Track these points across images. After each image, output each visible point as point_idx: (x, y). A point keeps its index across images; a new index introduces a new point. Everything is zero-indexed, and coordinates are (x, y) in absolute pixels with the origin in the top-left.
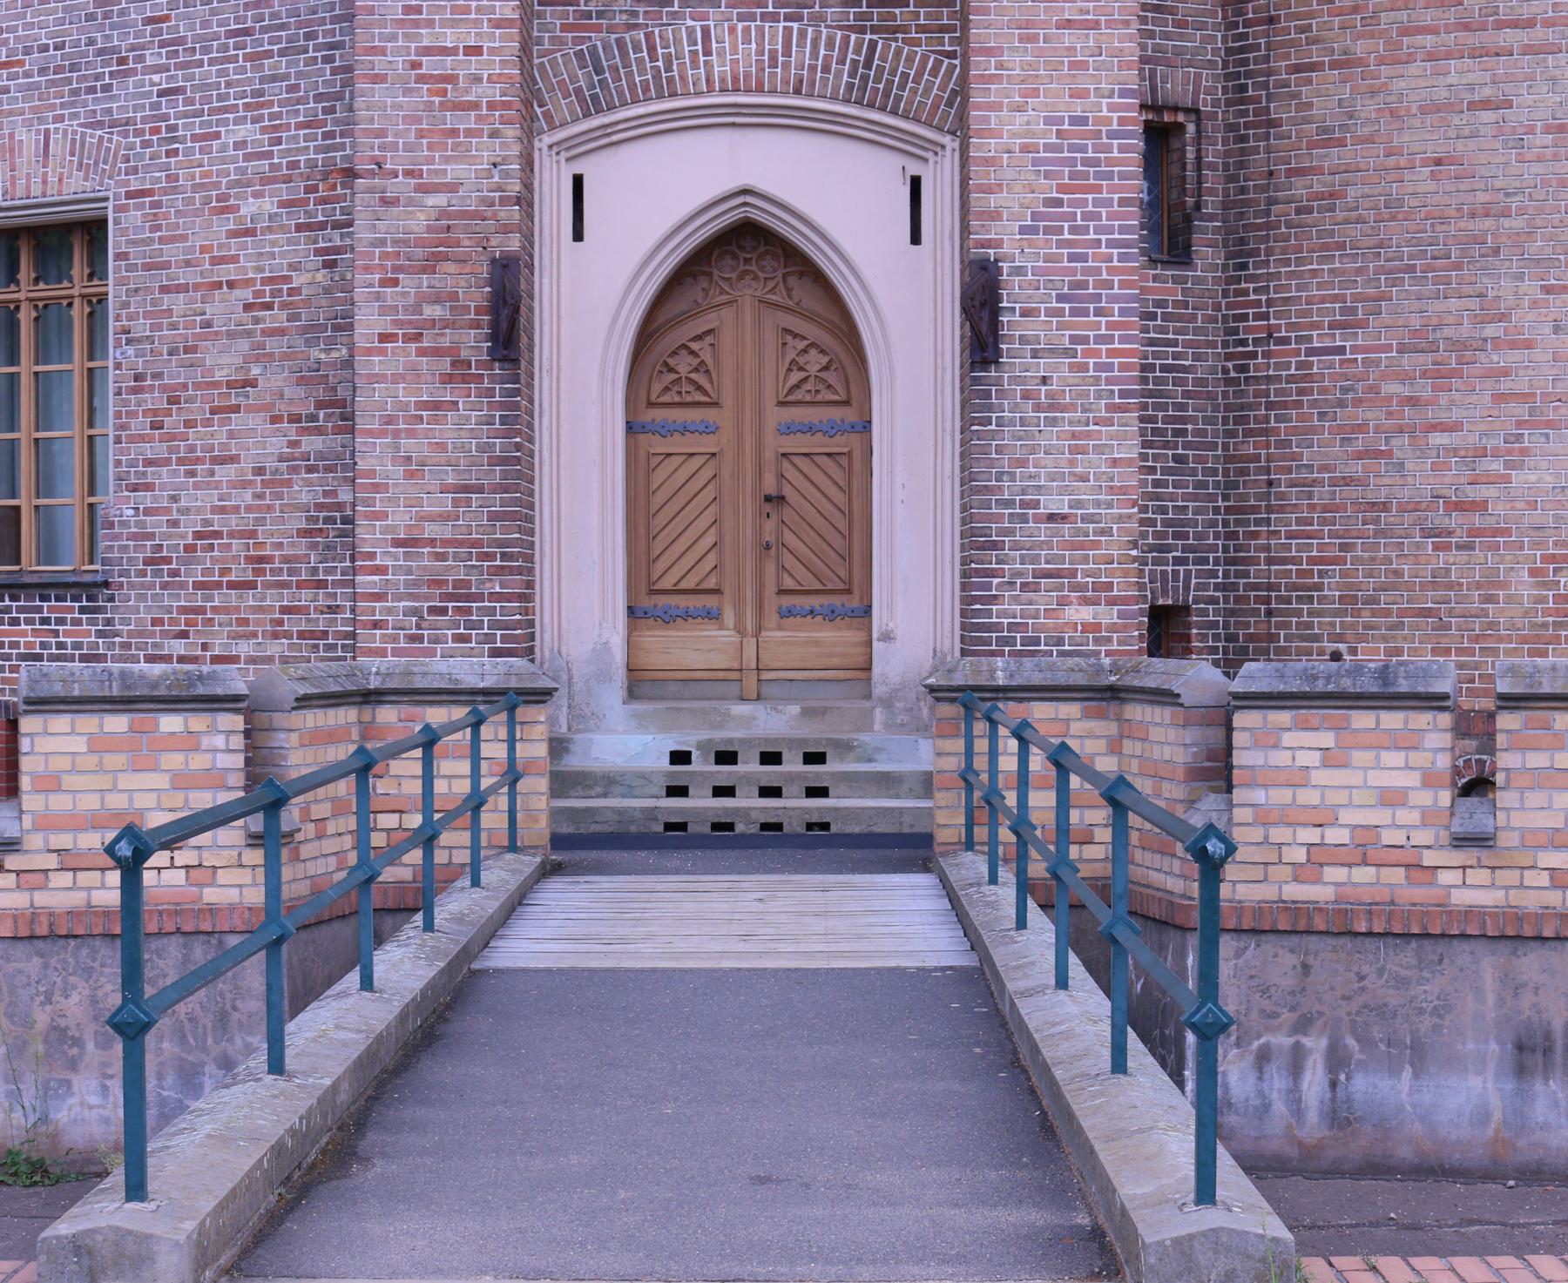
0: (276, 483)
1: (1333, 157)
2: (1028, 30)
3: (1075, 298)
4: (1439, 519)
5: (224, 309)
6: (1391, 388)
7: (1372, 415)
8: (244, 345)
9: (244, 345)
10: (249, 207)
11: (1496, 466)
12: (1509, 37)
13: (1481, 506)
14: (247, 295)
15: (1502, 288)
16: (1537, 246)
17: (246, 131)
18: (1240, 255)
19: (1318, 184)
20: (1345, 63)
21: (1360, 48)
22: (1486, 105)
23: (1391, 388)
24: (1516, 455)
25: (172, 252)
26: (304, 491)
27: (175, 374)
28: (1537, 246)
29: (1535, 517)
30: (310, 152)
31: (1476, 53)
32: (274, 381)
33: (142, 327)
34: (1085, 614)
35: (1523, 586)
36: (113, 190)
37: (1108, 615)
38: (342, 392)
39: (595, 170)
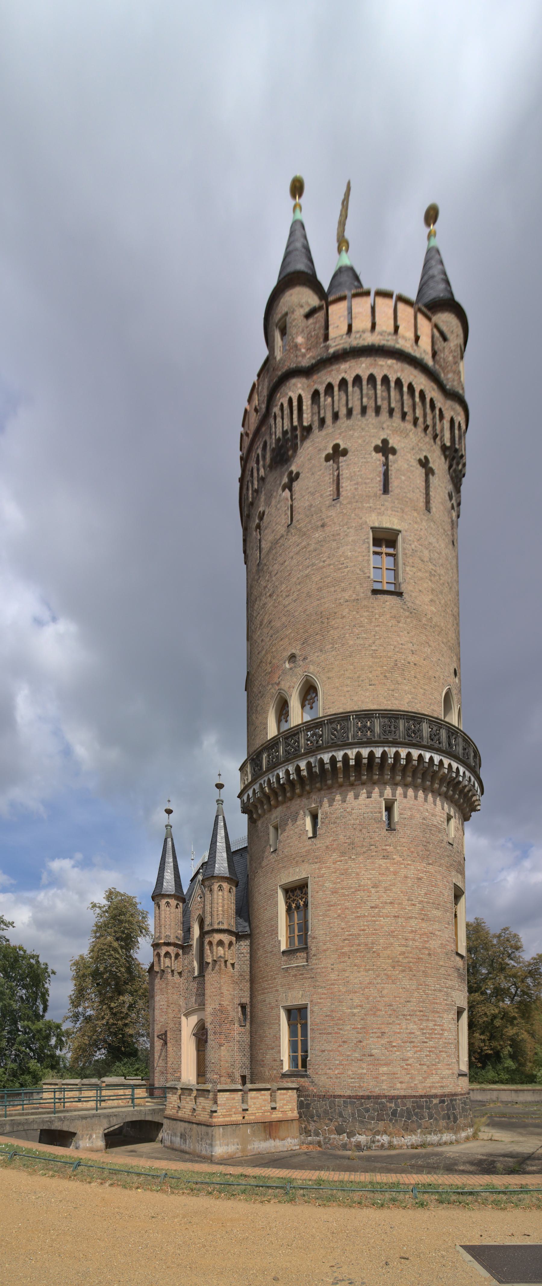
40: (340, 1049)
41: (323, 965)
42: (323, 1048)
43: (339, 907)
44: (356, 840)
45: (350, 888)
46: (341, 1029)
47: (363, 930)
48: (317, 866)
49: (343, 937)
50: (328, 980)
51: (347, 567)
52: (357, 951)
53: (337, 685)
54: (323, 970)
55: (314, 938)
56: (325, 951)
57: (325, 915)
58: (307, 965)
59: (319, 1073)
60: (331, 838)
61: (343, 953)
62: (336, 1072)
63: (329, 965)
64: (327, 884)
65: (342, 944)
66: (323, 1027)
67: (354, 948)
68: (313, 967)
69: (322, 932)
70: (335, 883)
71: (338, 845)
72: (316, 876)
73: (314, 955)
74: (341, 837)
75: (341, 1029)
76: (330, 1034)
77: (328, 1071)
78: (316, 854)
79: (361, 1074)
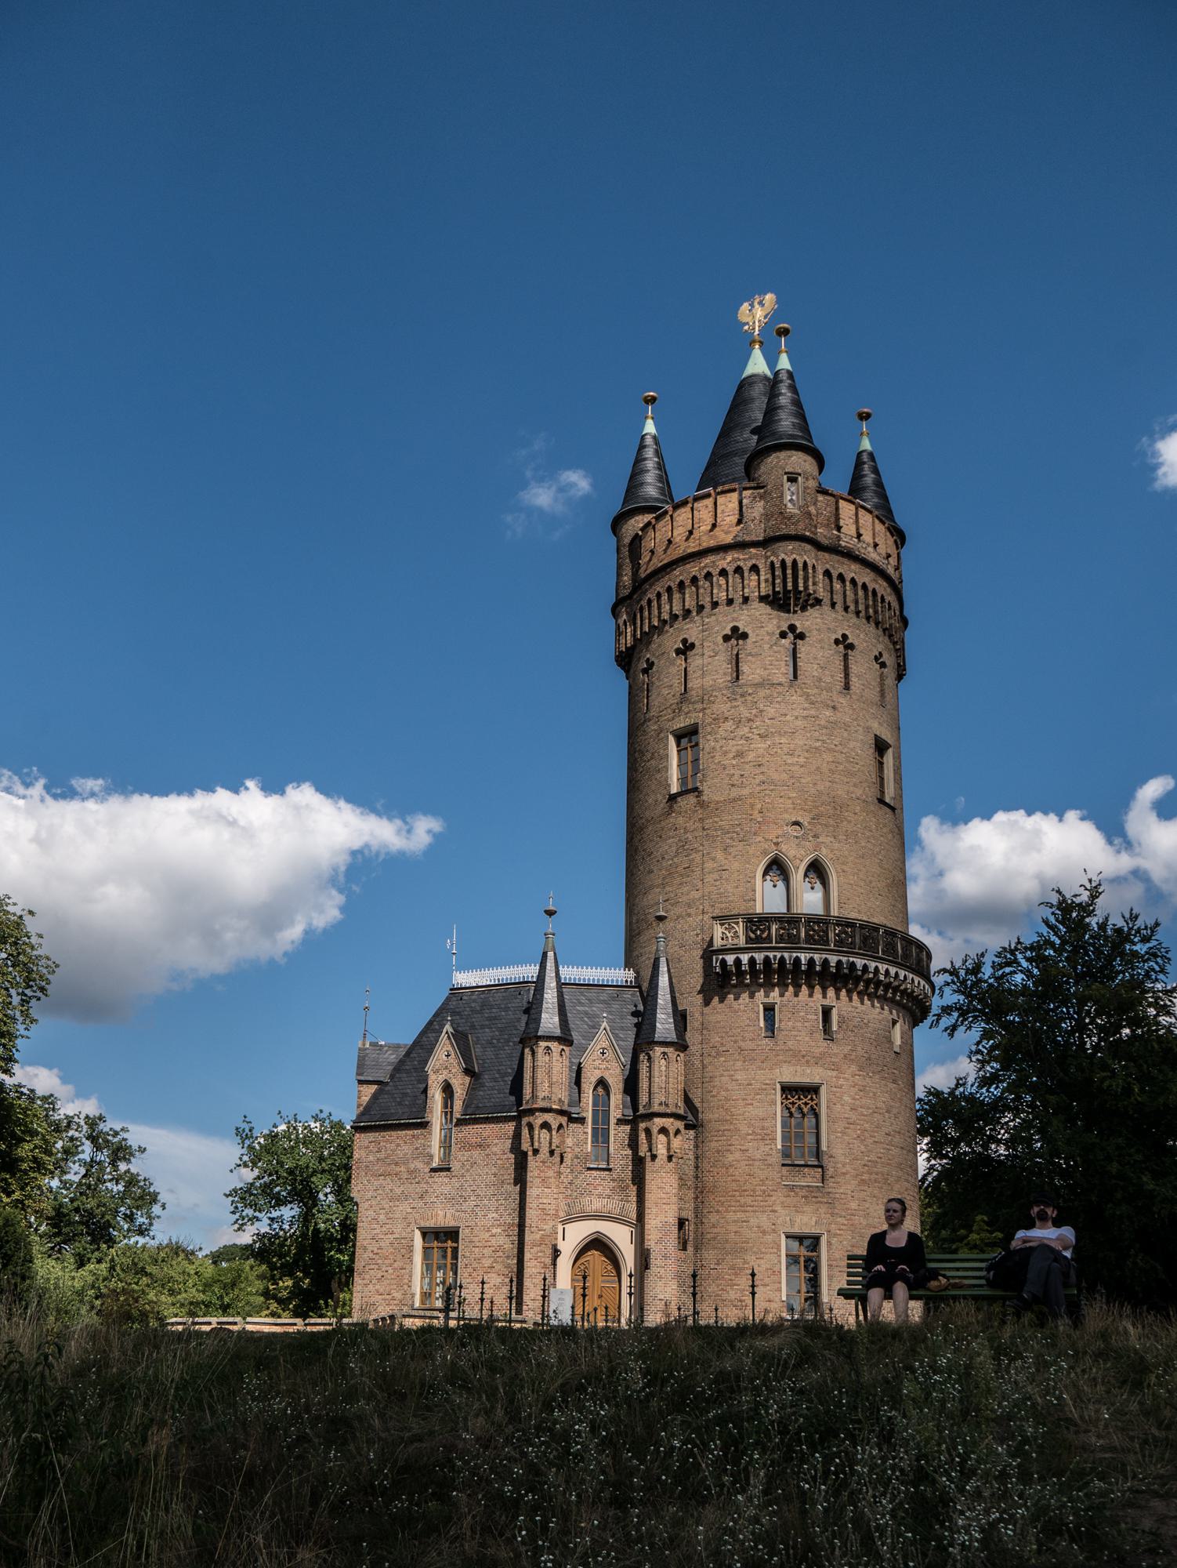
1: (715, 1230)
2: (656, 1204)
4: (736, 1303)
5: (487, 1252)
10: (494, 1231)
16: (755, 1249)
18: (697, 1249)
20: (718, 1211)
22: (745, 1221)
25: (475, 1239)
27: (475, 1265)
28: (755, 1249)
32: (498, 1267)
33: (468, 1254)
36: (461, 1225)
41: (842, 1191)
43: (859, 1127)
44: (873, 1056)
45: (869, 1108)
47: (881, 1158)
48: (834, 1073)
49: (863, 1162)
51: (857, 764)
52: (876, 1181)
54: (843, 1196)
55: (831, 1157)
56: (844, 1174)
57: (843, 1133)
61: (863, 1180)
64: (846, 1098)
67: (874, 1176)
68: (830, 1190)
69: (841, 1151)
71: (857, 1056)
73: (832, 1177)
74: (859, 1049)
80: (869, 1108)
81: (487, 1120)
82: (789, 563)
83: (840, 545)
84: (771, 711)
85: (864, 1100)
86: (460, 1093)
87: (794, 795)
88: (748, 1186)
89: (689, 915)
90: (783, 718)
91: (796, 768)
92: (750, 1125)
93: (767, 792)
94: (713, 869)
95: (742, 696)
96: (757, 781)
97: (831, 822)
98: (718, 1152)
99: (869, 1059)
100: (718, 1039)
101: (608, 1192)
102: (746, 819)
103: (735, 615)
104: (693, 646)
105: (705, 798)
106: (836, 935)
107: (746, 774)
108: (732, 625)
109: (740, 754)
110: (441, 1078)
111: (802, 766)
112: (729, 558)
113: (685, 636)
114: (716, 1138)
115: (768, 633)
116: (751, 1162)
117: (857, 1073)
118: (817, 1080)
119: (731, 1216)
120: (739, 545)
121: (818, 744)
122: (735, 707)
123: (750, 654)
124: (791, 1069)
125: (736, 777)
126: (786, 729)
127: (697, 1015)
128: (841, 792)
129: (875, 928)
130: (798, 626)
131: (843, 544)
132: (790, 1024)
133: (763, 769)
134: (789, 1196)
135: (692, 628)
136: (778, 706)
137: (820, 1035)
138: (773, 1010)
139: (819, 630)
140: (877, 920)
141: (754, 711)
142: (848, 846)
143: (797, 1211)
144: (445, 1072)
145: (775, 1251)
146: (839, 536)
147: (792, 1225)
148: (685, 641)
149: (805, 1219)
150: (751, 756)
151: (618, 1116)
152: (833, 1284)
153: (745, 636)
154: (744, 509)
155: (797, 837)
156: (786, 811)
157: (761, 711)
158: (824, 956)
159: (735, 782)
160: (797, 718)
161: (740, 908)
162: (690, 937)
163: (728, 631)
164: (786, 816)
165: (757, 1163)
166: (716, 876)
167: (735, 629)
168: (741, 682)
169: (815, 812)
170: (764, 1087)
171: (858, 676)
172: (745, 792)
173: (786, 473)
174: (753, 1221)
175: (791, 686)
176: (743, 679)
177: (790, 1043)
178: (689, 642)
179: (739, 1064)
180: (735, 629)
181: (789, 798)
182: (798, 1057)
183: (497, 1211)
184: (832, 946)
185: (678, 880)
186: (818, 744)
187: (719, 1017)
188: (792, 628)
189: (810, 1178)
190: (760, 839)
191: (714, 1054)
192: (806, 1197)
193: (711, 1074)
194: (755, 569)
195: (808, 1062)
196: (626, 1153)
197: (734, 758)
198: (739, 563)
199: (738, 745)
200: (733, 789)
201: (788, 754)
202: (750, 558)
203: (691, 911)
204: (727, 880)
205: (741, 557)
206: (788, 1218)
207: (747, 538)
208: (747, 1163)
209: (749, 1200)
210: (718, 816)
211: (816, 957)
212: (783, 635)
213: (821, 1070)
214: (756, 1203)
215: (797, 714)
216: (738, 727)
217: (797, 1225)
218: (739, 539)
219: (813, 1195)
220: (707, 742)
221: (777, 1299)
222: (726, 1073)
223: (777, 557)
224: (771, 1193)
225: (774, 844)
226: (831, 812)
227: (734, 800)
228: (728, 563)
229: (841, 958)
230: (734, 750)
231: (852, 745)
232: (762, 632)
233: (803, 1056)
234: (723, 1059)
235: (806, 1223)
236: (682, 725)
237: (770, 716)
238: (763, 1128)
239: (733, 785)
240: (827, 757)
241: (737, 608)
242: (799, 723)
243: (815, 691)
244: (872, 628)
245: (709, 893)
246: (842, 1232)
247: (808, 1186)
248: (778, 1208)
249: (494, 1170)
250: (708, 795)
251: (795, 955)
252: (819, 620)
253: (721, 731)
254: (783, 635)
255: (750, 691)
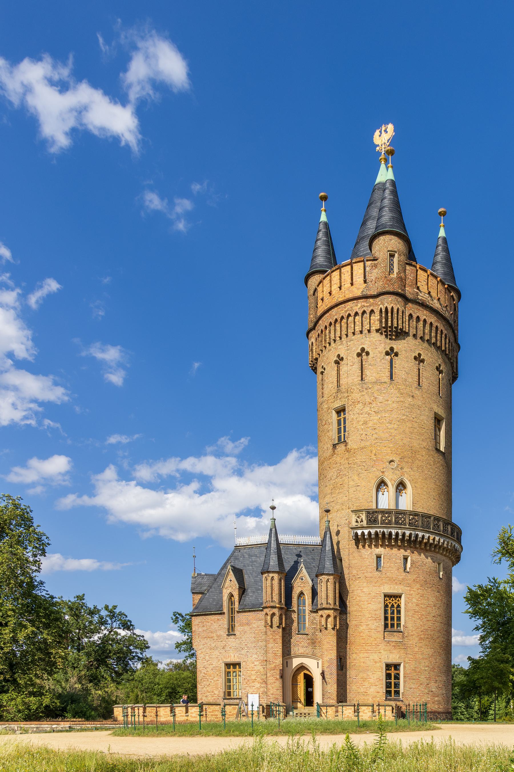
0: (259, 689)
1: (355, 661)
3: (331, 674)
4: (364, 693)
6: (360, 682)
7: (358, 684)
8: (255, 676)
9: (255, 676)
10: (256, 663)
11: (368, 689)
12: (369, 651)
13: (367, 692)
14: (256, 671)
15: (369, 673)
17: (256, 656)
19: (354, 664)
21: (357, 652)
23: (360, 682)
24: (370, 688)
25: (248, 667)
26: (262, 690)
29: (371, 694)
30: (262, 658)
31: (367, 653)
32: (258, 679)
34: (332, 701)
35: (371, 699)
37: (334, 701)
38: (265, 681)
39: (288, 660)
40: (419, 687)
42: (411, 686)
43: (420, 613)
46: (420, 677)
48: (409, 588)
49: (421, 630)
50: (413, 651)
53: (420, 492)
54: (411, 645)
55: (406, 627)
56: (412, 635)
58: (402, 641)
59: (409, 699)
60: (416, 576)
62: (417, 699)
63: (415, 644)
64: (414, 600)
65: (421, 633)
66: (411, 675)
69: (411, 625)
70: (417, 600)
71: (420, 580)
72: (408, 594)
73: (406, 637)
74: (421, 576)
75: (420, 677)
76: (415, 679)
77: (413, 699)
78: (408, 582)
79: (428, 701)
80: (425, 605)
81: (250, 611)
82: (389, 310)
83: (418, 299)
84: (381, 398)
85: (422, 601)
86: (236, 598)
87: (392, 446)
88: (369, 642)
89: (342, 509)
90: (386, 403)
91: (393, 431)
92: (370, 613)
93: (378, 444)
94: (353, 485)
95: (366, 389)
96: (374, 438)
97: (410, 461)
98: (356, 625)
99: (426, 581)
100: (356, 572)
101: (306, 645)
102: (368, 458)
103: (363, 341)
104: (342, 359)
105: (349, 447)
106: (410, 520)
107: (368, 434)
108: (361, 347)
109: (365, 423)
110: (228, 592)
111: (396, 430)
112: (359, 305)
113: (339, 353)
114: (355, 619)
115: (379, 352)
116: (370, 630)
117: (420, 588)
118: (400, 592)
119: (361, 655)
120: (365, 297)
121: (404, 417)
122: (363, 395)
123: (370, 365)
124: (389, 586)
125: (364, 435)
126: (388, 408)
127: (346, 560)
128: (415, 444)
129: (429, 516)
130: (395, 348)
131: (420, 298)
132: (388, 564)
133: (376, 431)
134: (387, 646)
135: (342, 348)
136: (384, 395)
137: (402, 570)
138: (381, 557)
139: (406, 351)
140: (431, 513)
141: (372, 398)
142: (418, 473)
143: (390, 653)
144: (230, 589)
145: (381, 670)
146: (417, 293)
147: (388, 659)
148: (339, 356)
149: (394, 656)
150: (370, 424)
151: (310, 609)
152: (406, 685)
153: (368, 354)
154: (367, 274)
155: (393, 469)
156: (387, 454)
157: (376, 398)
158: (403, 531)
159: (363, 438)
160: (393, 402)
161: (366, 506)
162: (343, 522)
163: (359, 351)
164: (388, 457)
165: (373, 631)
166: (354, 489)
167: (363, 350)
168: (366, 381)
169: (402, 455)
170: (376, 595)
171: (427, 378)
172: (368, 444)
173: (388, 251)
174: (371, 657)
175: (391, 384)
176: (367, 379)
177: (388, 574)
178: (341, 357)
179: (365, 584)
180: (363, 350)
181: (389, 447)
182: (392, 580)
183: (256, 654)
184: (407, 526)
185: (337, 491)
186: (404, 417)
187: (356, 561)
188: (392, 349)
189: (396, 638)
190: (375, 469)
191: (354, 579)
192: (394, 646)
193: (353, 589)
194: (372, 311)
195: (396, 583)
196: (314, 626)
197: (362, 424)
198: (364, 308)
199: (364, 417)
200: (362, 442)
201: (389, 423)
202: (370, 306)
203: (344, 507)
204: (359, 491)
205: (366, 305)
206: (386, 656)
207: (369, 293)
208: (368, 631)
209: (369, 648)
210: (354, 456)
211: (400, 531)
212: (387, 354)
213: (402, 587)
214: (372, 649)
215: (394, 400)
216: (364, 407)
217: (390, 659)
218: (364, 293)
219: (398, 645)
220: (349, 416)
221: (381, 692)
222: (359, 589)
223: (383, 305)
224: (379, 644)
225: (382, 472)
226: (410, 455)
227: (362, 448)
228: (359, 309)
229: (412, 532)
230: (362, 420)
231: (422, 418)
232: (376, 351)
233: (394, 580)
234: (358, 582)
235: (393, 659)
236: (338, 406)
237: (380, 401)
238: (376, 615)
239: (362, 440)
240: (409, 424)
241: (364, 337)
242: (395, 405)
243: (404, 387)
244: (433, 349)
245: (351, 498)
246: (410, 662)
247: (396, 641)
248: (382, 651)
249: (254, 635)
250: (351, 444)
251: (389, 530)
252: (406, 345)
253: (356, 410)
254: (387, 354)
255: (370, 387)
